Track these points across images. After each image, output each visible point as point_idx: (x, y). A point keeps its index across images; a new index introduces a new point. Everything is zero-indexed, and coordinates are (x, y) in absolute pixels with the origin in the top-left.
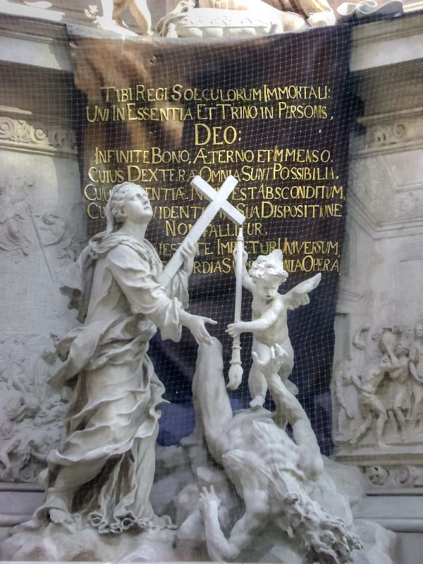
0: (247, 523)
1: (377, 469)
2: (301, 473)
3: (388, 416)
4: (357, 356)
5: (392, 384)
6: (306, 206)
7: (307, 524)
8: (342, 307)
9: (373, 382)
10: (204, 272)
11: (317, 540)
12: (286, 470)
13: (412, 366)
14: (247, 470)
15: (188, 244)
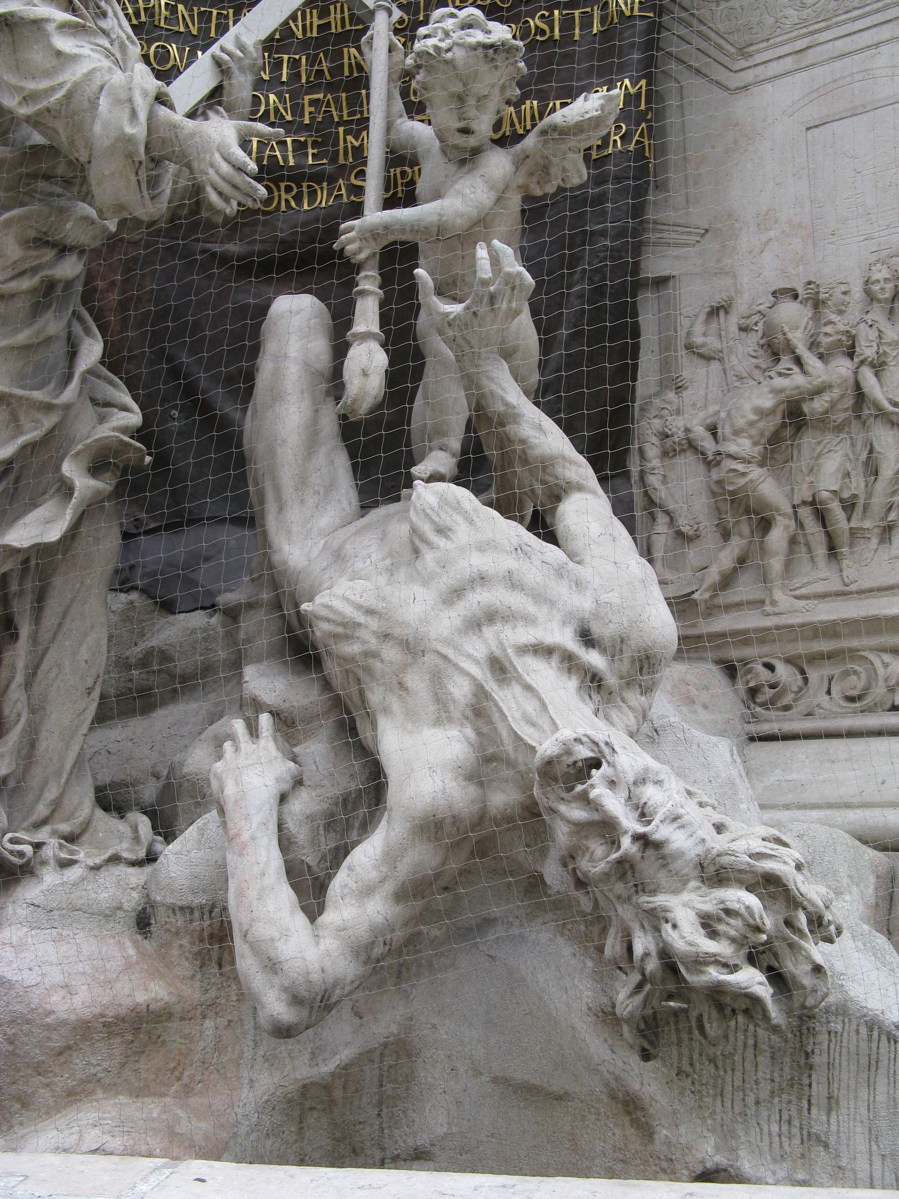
0: (391, 857)
1: (770, 667)
2: (595, 659)
3: (800, 525)
4: (701, 378)
5: (808, 440)
6: (556, 12)
7: (649, 868)
8: (654, 265)
9: (753, 432)
10: (306, 207)
11: (687, 936)
12: (544, 651)
13: (868, 377)
14: (391, 653)
15: (237, 38)
